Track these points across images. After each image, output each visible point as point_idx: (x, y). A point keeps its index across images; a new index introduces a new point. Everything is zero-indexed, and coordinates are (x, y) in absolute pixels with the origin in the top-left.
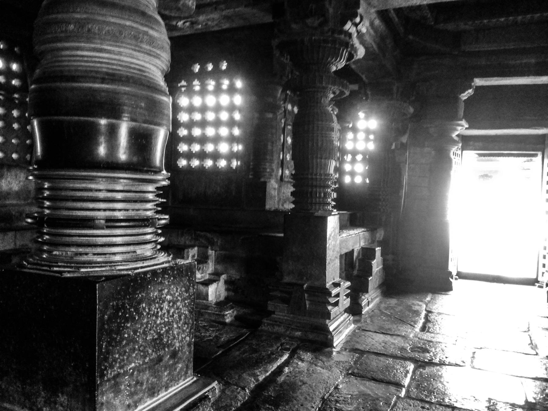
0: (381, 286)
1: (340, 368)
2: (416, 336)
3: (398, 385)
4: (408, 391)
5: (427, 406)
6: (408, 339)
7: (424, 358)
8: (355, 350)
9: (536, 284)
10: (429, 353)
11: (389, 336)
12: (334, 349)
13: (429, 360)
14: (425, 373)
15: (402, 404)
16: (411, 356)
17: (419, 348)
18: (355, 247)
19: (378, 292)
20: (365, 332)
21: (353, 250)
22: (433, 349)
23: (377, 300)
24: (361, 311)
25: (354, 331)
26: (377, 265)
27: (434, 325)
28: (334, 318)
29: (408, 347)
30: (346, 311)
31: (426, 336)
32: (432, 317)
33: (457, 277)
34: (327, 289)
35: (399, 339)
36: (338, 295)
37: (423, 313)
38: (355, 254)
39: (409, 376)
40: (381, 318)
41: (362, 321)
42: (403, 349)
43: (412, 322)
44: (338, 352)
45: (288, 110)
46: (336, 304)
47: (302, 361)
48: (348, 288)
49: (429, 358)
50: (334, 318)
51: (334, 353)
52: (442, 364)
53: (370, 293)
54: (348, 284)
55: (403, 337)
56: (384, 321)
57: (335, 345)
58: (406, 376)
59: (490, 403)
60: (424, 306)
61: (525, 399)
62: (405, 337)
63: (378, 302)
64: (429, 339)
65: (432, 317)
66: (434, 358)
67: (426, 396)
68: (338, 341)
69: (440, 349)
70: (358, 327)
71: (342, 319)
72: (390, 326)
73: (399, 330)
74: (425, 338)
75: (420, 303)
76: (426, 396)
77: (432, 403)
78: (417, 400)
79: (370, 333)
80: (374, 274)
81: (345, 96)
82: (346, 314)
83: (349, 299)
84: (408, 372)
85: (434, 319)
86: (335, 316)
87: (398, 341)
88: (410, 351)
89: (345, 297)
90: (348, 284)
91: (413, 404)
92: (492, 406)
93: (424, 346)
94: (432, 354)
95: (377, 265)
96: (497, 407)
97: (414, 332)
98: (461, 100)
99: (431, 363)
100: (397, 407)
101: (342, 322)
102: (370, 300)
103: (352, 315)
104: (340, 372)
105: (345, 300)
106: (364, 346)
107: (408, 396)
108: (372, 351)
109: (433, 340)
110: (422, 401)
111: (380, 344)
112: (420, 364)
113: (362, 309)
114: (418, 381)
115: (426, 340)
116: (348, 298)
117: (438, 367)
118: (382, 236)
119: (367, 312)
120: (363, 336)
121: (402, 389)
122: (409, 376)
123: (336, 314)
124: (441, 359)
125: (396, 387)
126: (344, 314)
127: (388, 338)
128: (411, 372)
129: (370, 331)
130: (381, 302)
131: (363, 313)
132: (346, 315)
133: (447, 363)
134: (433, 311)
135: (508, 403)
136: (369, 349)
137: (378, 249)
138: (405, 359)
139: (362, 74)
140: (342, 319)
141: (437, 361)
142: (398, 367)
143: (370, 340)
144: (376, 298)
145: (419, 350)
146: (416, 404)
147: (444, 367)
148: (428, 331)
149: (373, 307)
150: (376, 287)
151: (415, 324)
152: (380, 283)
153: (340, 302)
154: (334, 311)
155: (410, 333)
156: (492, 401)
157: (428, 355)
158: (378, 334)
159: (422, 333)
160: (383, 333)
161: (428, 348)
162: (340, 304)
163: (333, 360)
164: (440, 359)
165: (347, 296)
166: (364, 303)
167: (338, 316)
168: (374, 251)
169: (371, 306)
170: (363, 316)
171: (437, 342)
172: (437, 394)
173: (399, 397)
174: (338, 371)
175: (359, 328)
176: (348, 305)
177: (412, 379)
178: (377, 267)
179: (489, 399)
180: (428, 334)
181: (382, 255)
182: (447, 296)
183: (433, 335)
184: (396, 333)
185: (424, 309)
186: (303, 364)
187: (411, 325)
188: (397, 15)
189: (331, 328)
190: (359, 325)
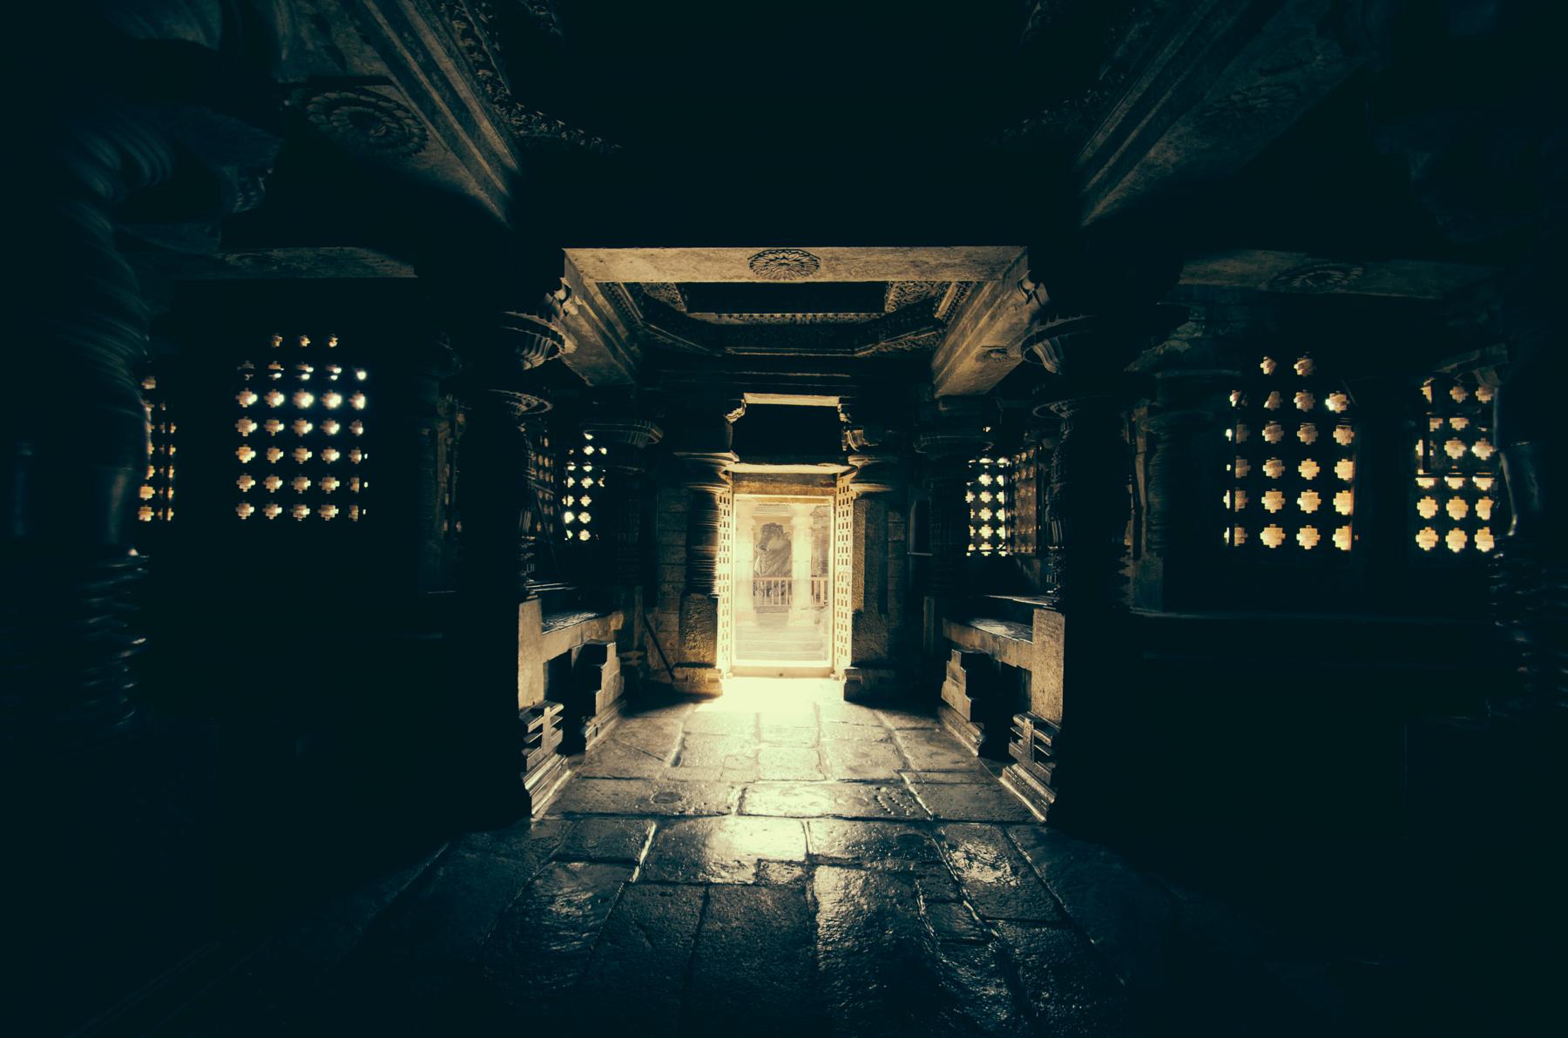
0: (617, 701)
1: (538, 852)
2: (663, 776)
3: (631, 863)
4: (643, 870)
5: (670, 891)
6: (653, 781)
7: (674, 810)
8: (569, 815)
9: (832, 675)
10: (680, 800)
11: (624, 782)
12: (532, 820)
13: (680, 812)
14: (671, 835)
15: (631, 896)
16: (654, 810)
17: (667, 794)
18: (574, 644)
19: (614, 711)
20: (587, 781)
21: (570, 651)
22: (688, 794)
23: (612, 724)
24: (585, 747)
25: (570, 781)
26: (610, 670)
27: (692, 754)
28: (533, 768)
29: (650, 795)
30: (561, 750)
31: (679, 773)
32: (692, 741)
33: (731, 674)
34: (520, 721)
35: (640, 783)
36: (540, 729)
37: (680, 736)
38: (574, 656)
39: (648, 844)
40: (614, 753)
41: (586, 761)
42: (644, 800)
43: (661, 753)
44: (541, 823)
45: (459, 425)
46: (538, 743)
47: (472, 849)
48: (559, 714)
49: (680, 809)
50: (533, 768)
51: (532, 827)
52: (698, 815)
53: (599, 716)
54: (560, 707)
55: (644, 779)
56: (620, 758)
57: (533, 812)
58: (643, 845)
59: (759, 867)
60: (681, 725)
61: (805, 851)
62: (647, 780)
63: (613, 727)
64: (683, 778)
65: (690, 741)
66: (687, 807)
67: (670, 874)
68: (540, 805)
69: (697, 792)
70: (576, 773)
71: (549, 764)
72: (627, 765)
73: (639, 769)
74: (678, 777)
75: (675, 721)
76: (670, 874)
77: (678, 884)
78: (656, 883)
79: (595, 781)
80: (603, 685)
81: (547, 410)
82: (556, 755)
83: (561, 732)
84: (646, 838)
85: (693, 744)
86: (535, 763)
87: (635, 788)
88: (652, 802)
89: (554, 729)
90: (560, 707)
91: (649, 890)
92: (763, 870)
93: (674, 790)
94: (685, 801)
95: (610, 670)
96: (768, 872)
97: (663, 769)
98: (729, 422)
99: (683, 817)
100: (623, 903)
101: (548, 771)
102: (599, 726)
103: (567, 756)
104: (536, 859)
105: (553, 734)
106: (583, 805)
107: (643, 880)
108: (594, 811)
109: (689, 778)
110: (663, 882)
111: (608, 797)
112: (665, 820)
113: (586, 742)
114: (661, 851)
115: (679, 780)
116: (559, 729)
117: (692, 822)
118: (621, 623)
119: (595, 746)
120: (582, 790)
121: (634, 869)
122: (648, 844)
123: (536, 760)
124: (697, 807)
125: (623, 867)
126: (552, 757)
127: (623, 785)
128: (650, 838)
129: (595, 778)
130: (617, 727)
131: (587, 749)
132: (557, 757)
133: (705, 813)
134: (692, 731)
135: (783, 862)
136: (590, 809)
137: (612, 649)
138: (644, 816)
139: (584, 375)
140: (549, 764)
141: (691, 812)
142: (633, 832)
143: (594, 792)
144: (609, 721)
145: (666, 798)
146: (654, 891)
147: (700, 820)
148: (682, 766)
149: (603, 737)
150: (607, 704)
151: (665, 756)
152: (617, 696)
153: (544, 738)
154: (532, 756)
155: (656, 772)
156: (762, 864)
157: (679, 804)
158: (607, 781)
159: (674, 769)
160: (615, 778)
161: (681, 792)
162: (544, 743)
163: (527, 839)
164: (696, 809)
165: (557, 726)
166: (587, 734)
167: (540, 761)
168: (604, 650)
169: (600, 735)
170: (587, 755)
171: (693, 781)
172: (686, 867)
173: (628, 884)
174: (534, 857)
175: (578, 775)
176: (560, 740)
177: (651, 849)
178: (610, 674)
179: (759, 860)
180: (682, 769)
181: (619, 651)
182: (716, 701)
183: (689, 770)
184: (635, 775)
185: (681, 730)
186: (474, 856)
187: (659, 759)
188: (631, 292)
189: (527, 786)
190: (578, 769)
